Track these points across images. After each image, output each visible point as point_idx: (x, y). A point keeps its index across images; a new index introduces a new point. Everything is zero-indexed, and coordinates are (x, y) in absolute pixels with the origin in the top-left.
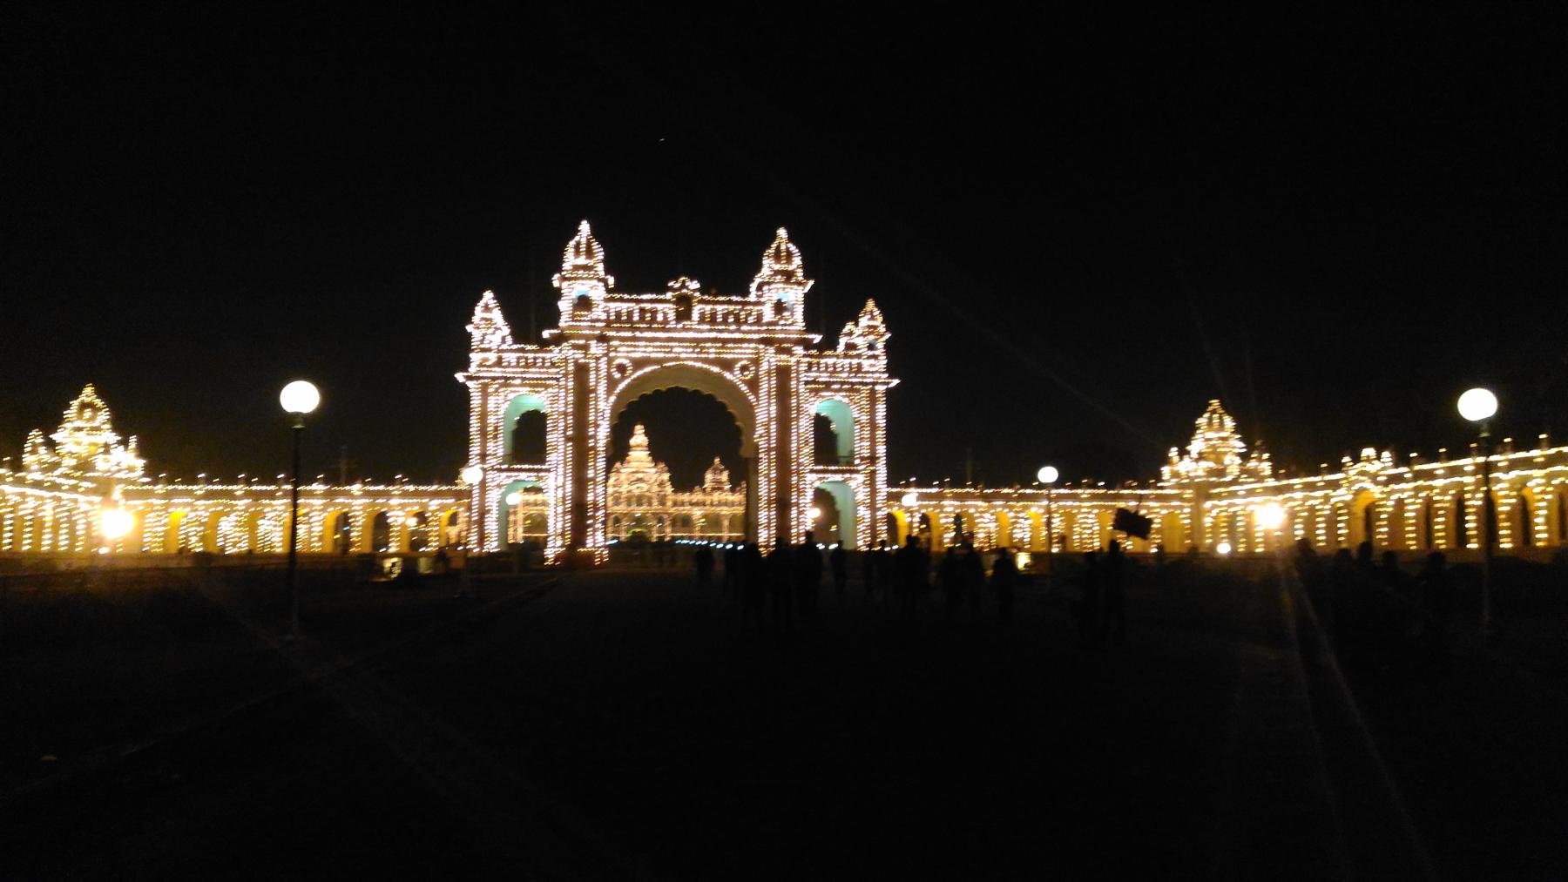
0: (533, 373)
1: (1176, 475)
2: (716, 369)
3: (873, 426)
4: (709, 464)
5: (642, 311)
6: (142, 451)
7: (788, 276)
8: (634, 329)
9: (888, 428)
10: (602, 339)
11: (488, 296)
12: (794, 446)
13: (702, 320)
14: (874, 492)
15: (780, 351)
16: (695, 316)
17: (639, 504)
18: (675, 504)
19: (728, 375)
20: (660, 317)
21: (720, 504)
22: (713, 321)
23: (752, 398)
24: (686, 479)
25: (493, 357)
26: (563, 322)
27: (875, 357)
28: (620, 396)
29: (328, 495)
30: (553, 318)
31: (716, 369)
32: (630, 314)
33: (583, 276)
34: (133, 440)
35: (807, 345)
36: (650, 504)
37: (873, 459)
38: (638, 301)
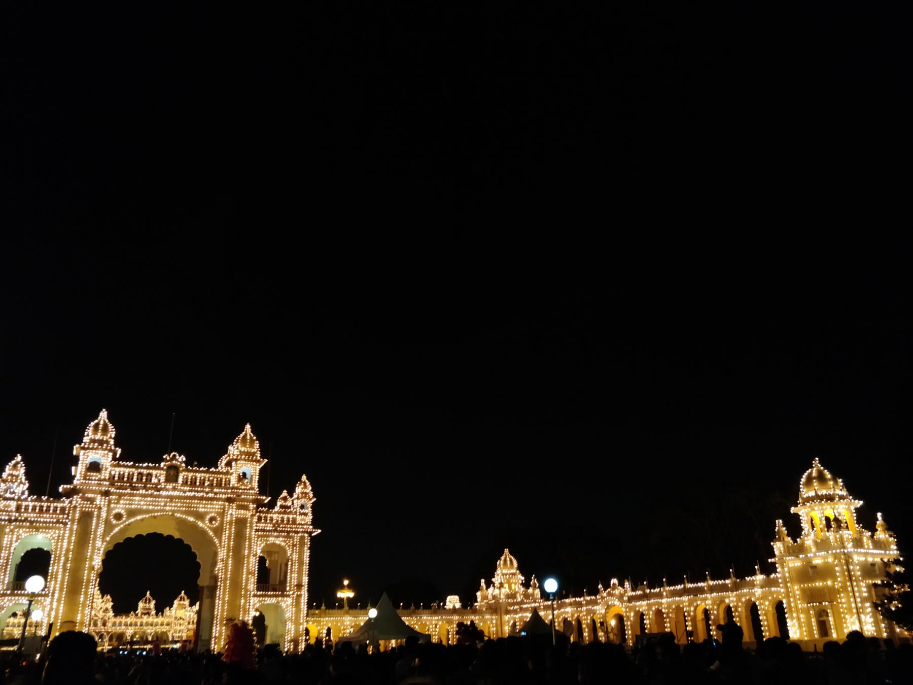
0: (46, 518)
1: (485, 597)
2: (191, 519)
4: (142, 596)
5: (140, 474)
8: (133, 488)
9: (311, 564)
13: (185, 483)
14: (298, 610)
15: (240, 507)
16: (180, 480)
18: (114, 624)
19: (200, 524)
20: (154, 480)
21: (147, 624)
22: (193, 483)
24: (123, 607)
27: (306, 514)
31: (191, 519)
32: (130, 477)
36: (95, 625)
37: (299, 586)
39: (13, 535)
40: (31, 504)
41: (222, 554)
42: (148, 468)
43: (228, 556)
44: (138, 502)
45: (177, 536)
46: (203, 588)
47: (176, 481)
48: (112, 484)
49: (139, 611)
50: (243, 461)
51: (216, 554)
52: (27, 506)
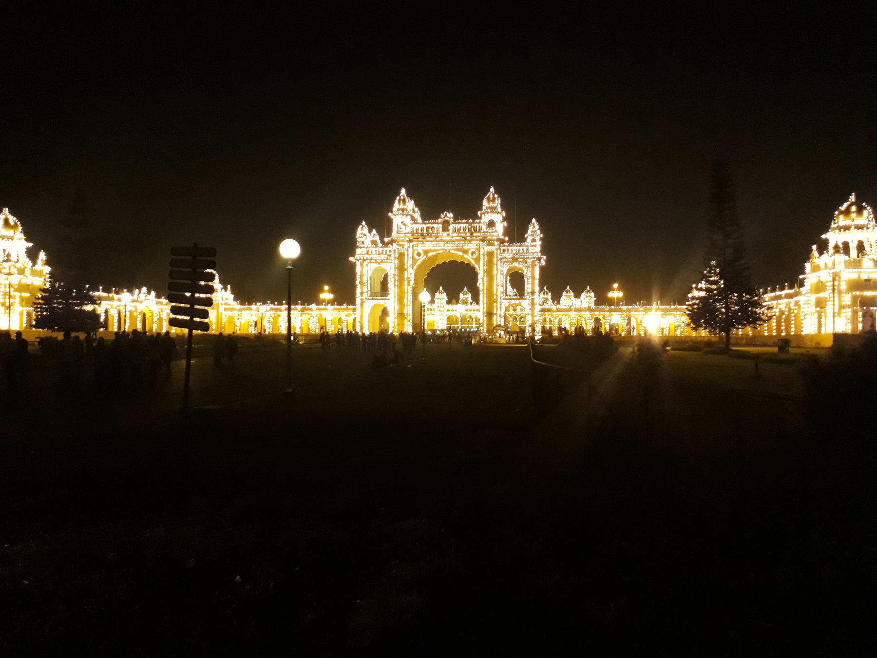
3: (533, 278)
6: (233, 292)
7: (493, 210)
12: (495, 288)
13: (454, 231)
15: (490, 244)
19: (466, 256)
23: (477, 266)
25: (365, 251)
26: (394, 234)
27: (535, 246)
28: (419, 267)
29: (303, 310)
30: (389, 233)
31: (460, 253)
33: (404, 213)
34: (229, 287)
35: (502, 242)
41: (480, 276)
44: (428, 246)
48: (413, 235)
50: (493, 214)
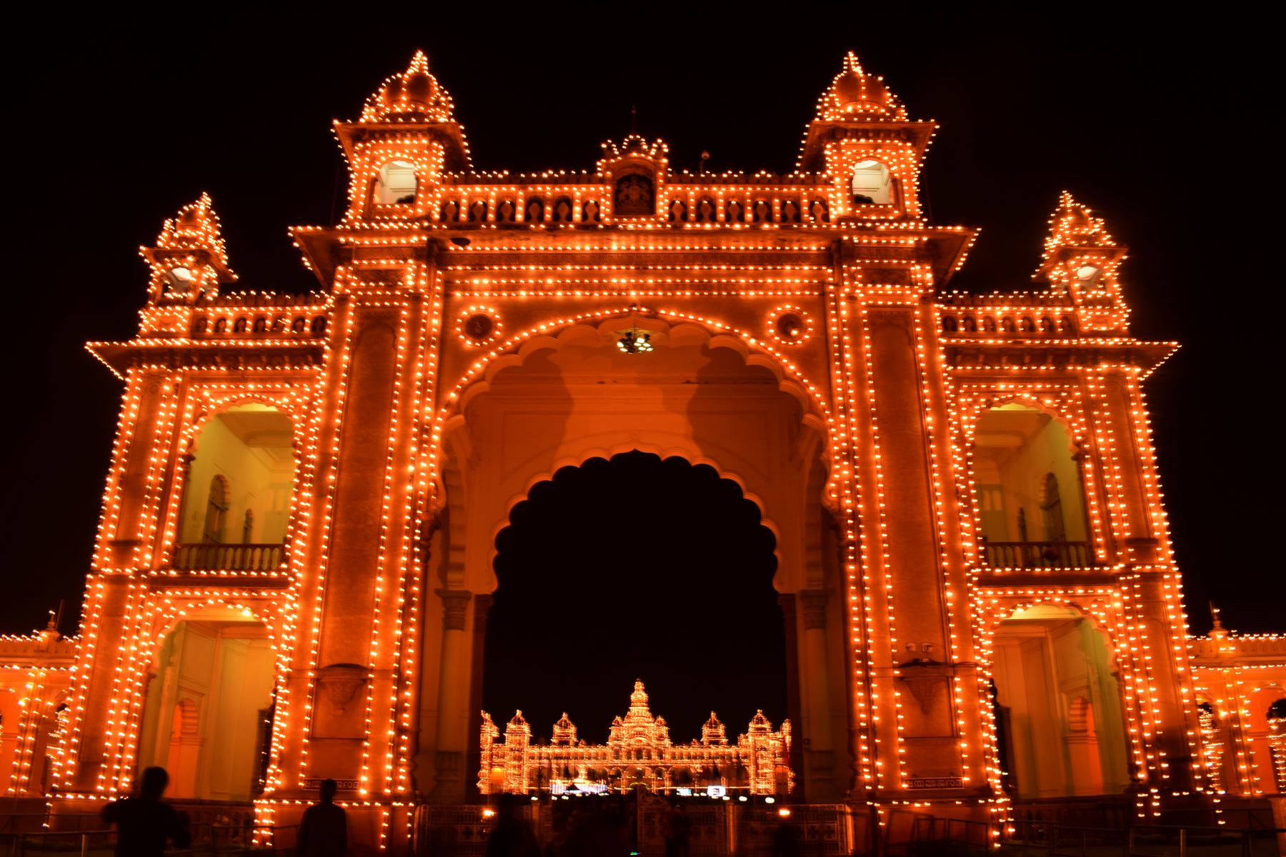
3: (1131, 464)
4: (705, 718)
10: (433, 255)
11: (205, 201)
14: (1159, 629)
15: (878, 275)
16: (662, 208)
17: (639, 756)
18: (673, 756)
24: (683, 732)
36: (649, 757)
37: (1143, 544)
38: (523, 184)
39: (181, 402)
40: (231, 313)
41: (840, 433)
42: (552, 181)
43: (864, 434)
45: (696, 457)
46: (790, 598)
47: (649, 208)
49: (704, 739)
51: (821, 442)
52: (221, 320)
